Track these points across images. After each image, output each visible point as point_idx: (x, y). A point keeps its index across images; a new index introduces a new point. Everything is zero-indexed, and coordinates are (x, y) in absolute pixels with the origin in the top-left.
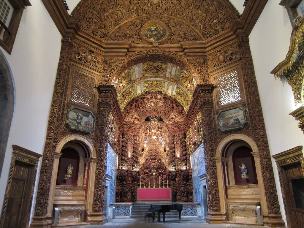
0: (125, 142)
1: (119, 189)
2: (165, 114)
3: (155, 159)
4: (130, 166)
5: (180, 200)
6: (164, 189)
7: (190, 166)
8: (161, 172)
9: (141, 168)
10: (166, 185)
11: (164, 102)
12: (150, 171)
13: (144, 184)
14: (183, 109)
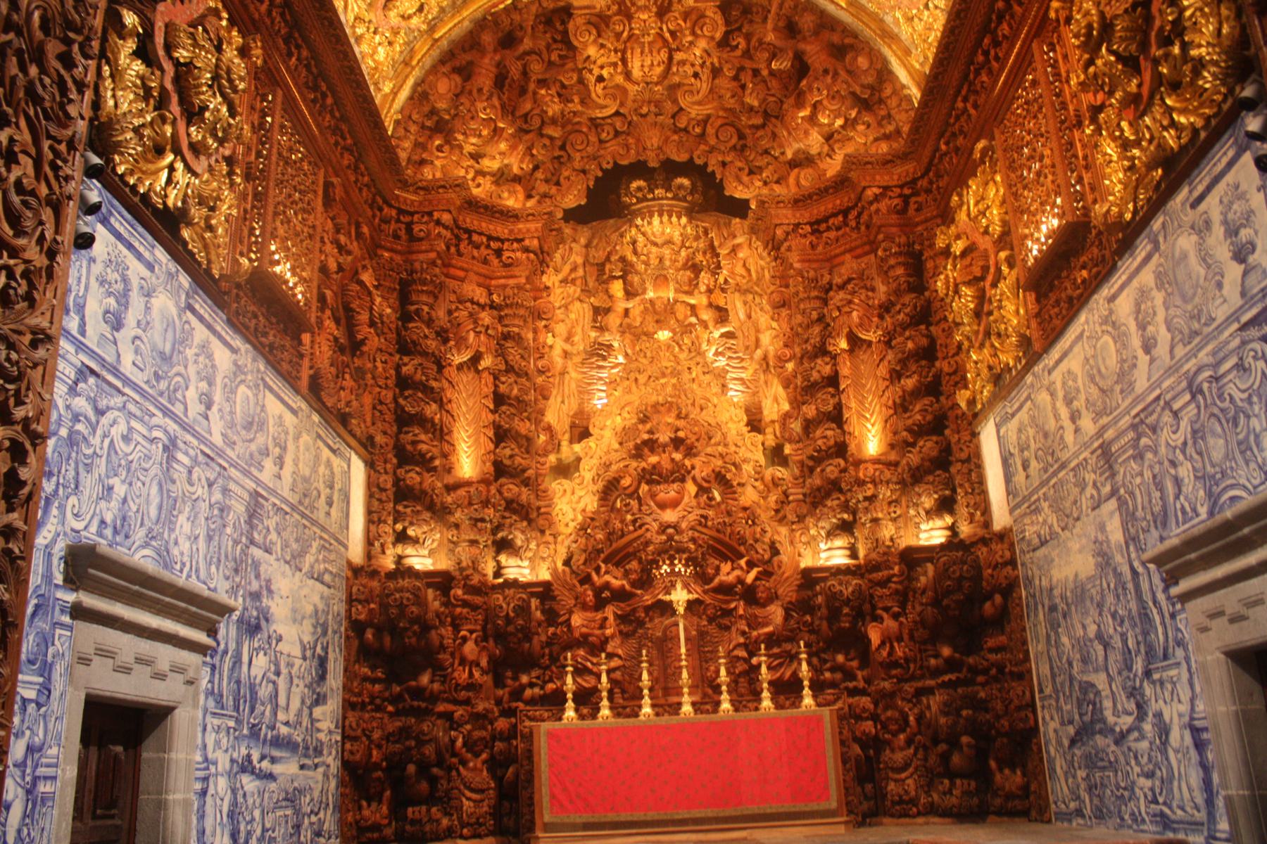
0: (424, 354)
1: (376, 735)
2: (741, 136)
3: (683, 480)
4: (473, 543)
5: (913, 801)
6: (771, 721)
7: (986, 510)
8: (740, 581)
9: (567, 563)
10: (787, 690)
11: (724, 43)
12: (645, 580)
13: (595, 691)
14: (885, 74)
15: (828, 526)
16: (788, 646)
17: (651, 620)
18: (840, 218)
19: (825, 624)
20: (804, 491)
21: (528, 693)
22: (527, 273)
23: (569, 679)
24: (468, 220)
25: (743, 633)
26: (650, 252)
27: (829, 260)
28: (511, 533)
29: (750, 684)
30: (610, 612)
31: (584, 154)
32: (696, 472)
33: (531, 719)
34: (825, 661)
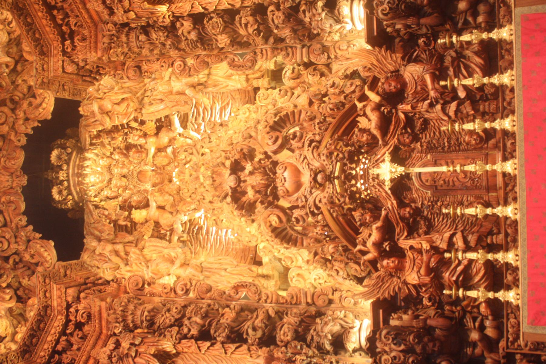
3: (275, 164)
8: (378, 107)
9: (360, 281)
13: (489, 264)
15: (331, 21)
16: (448, 60)
17: (414, 201)
18: (55, 12)
19: (423, 21)
20: (299, 46)
21: (490, 332)
22: (97, 300)
23: (473, 294)
24: (42, 354)
25: (431, 105)
26: (116, 186)
27: (96, 25)
28: (326, 336)
29: (487, 99)
30: (404, 243)
31: (13, 240)
32: (270, 149)
33: (517, 338)
34: (466, 22)
